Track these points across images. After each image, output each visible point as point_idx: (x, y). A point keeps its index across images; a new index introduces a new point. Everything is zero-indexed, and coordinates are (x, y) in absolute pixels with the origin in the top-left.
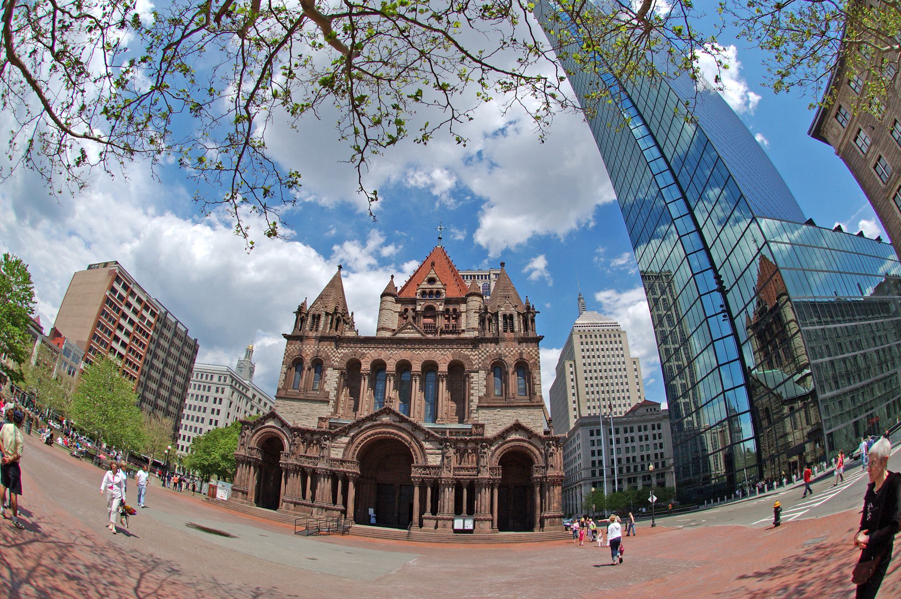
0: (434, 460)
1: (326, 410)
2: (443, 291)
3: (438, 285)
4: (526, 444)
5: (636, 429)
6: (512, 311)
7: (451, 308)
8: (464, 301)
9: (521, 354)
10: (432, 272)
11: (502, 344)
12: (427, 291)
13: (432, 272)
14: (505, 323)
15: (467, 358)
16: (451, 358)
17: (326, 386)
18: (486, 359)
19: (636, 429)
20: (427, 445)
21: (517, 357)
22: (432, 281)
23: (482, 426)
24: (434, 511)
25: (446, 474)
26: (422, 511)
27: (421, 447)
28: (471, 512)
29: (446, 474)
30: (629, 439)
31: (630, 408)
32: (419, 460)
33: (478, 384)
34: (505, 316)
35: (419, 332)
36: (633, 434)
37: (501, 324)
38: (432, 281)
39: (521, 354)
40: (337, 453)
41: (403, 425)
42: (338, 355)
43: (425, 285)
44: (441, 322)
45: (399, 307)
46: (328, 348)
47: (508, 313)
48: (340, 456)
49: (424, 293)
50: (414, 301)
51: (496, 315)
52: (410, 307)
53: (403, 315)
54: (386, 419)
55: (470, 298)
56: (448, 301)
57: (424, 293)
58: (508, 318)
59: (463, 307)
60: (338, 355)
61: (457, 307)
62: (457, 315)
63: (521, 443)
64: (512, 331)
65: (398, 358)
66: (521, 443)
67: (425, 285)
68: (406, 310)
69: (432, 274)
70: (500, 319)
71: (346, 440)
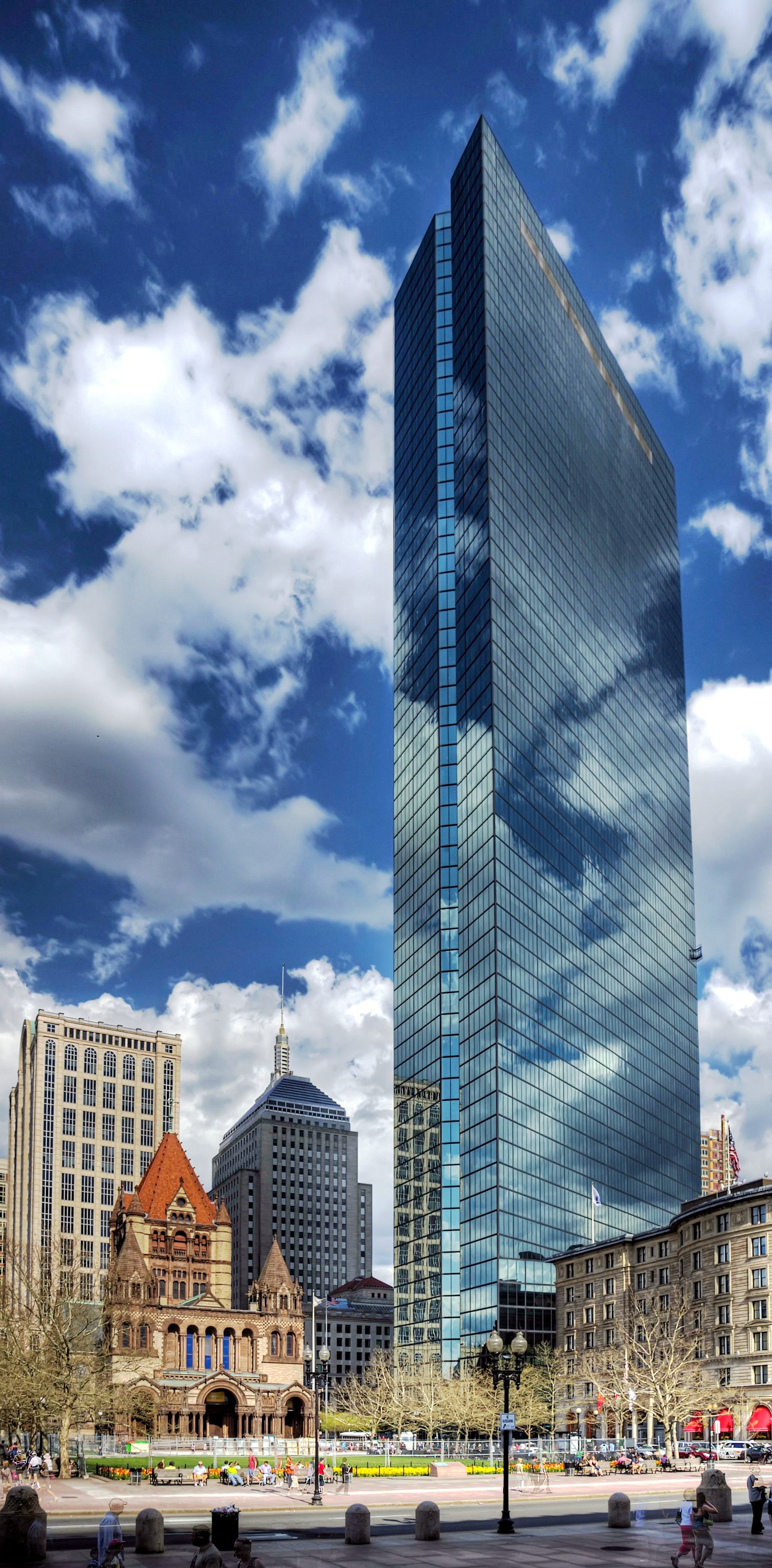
0: (251, 1402)
1: (157, 1363)
2: (194, 1216)
3: (188, 1209)
5: (354, 1328)
6: (287, 1293)
7: (201, 1233)
8: (214, 1229)
9: (291, 1327)
10: (182, 1191)
11: (279, 1319)
12: (178, 1213)
13: (182, 1191)
14: (281, 1302)
15: (255, 1326)
16: (243, 1327)
17: (154, 1346)
19: (354, 1328)
20: (248, 1393)
21: (288, 1329)
22: (182, 1201)
23: (266, 1376)
24: (250, 1432)
25: (259, 1412)
26: (244, 1432)
27: (244, 1395)
28: (270, 1432)
29: (259, 1412)
30: (343, 1342)
31: (344, 1282)
32: (241, 1402)
33: (263, 1345)
34: (281, 1296)
35: (217, 1300)
36: (349, 1336)
37: (278, 1303)
38: (182, 1201)
39: (291, 1327)
40: (192, 1401)
41: (232, 1381)
42: (161, 1319)
43: (174, 1207)
44: (190, 1250)
45: (148, 1229)
46: (151, 1315)
47: (284, 1294)
48: (195, 1403)
49: (174, 1214)
50: (164, 1224)
51: (276, 1293)
52: (160, 1228)
53: (154, 1236)
54: (220, 1377)
55: (220, 1228)
56: (198, 1228)
57: (174, 1214)
59: (213, 1236)
60: (161, 1319)
61: (208, 1233)
62: (208, 1243)
64: (286, 1308)
65: (208, 1325)
67: (174, 1207)
68: (156, 1232)
69: (182, 1193)
70: (278, 1299)
71: (196, 1391)
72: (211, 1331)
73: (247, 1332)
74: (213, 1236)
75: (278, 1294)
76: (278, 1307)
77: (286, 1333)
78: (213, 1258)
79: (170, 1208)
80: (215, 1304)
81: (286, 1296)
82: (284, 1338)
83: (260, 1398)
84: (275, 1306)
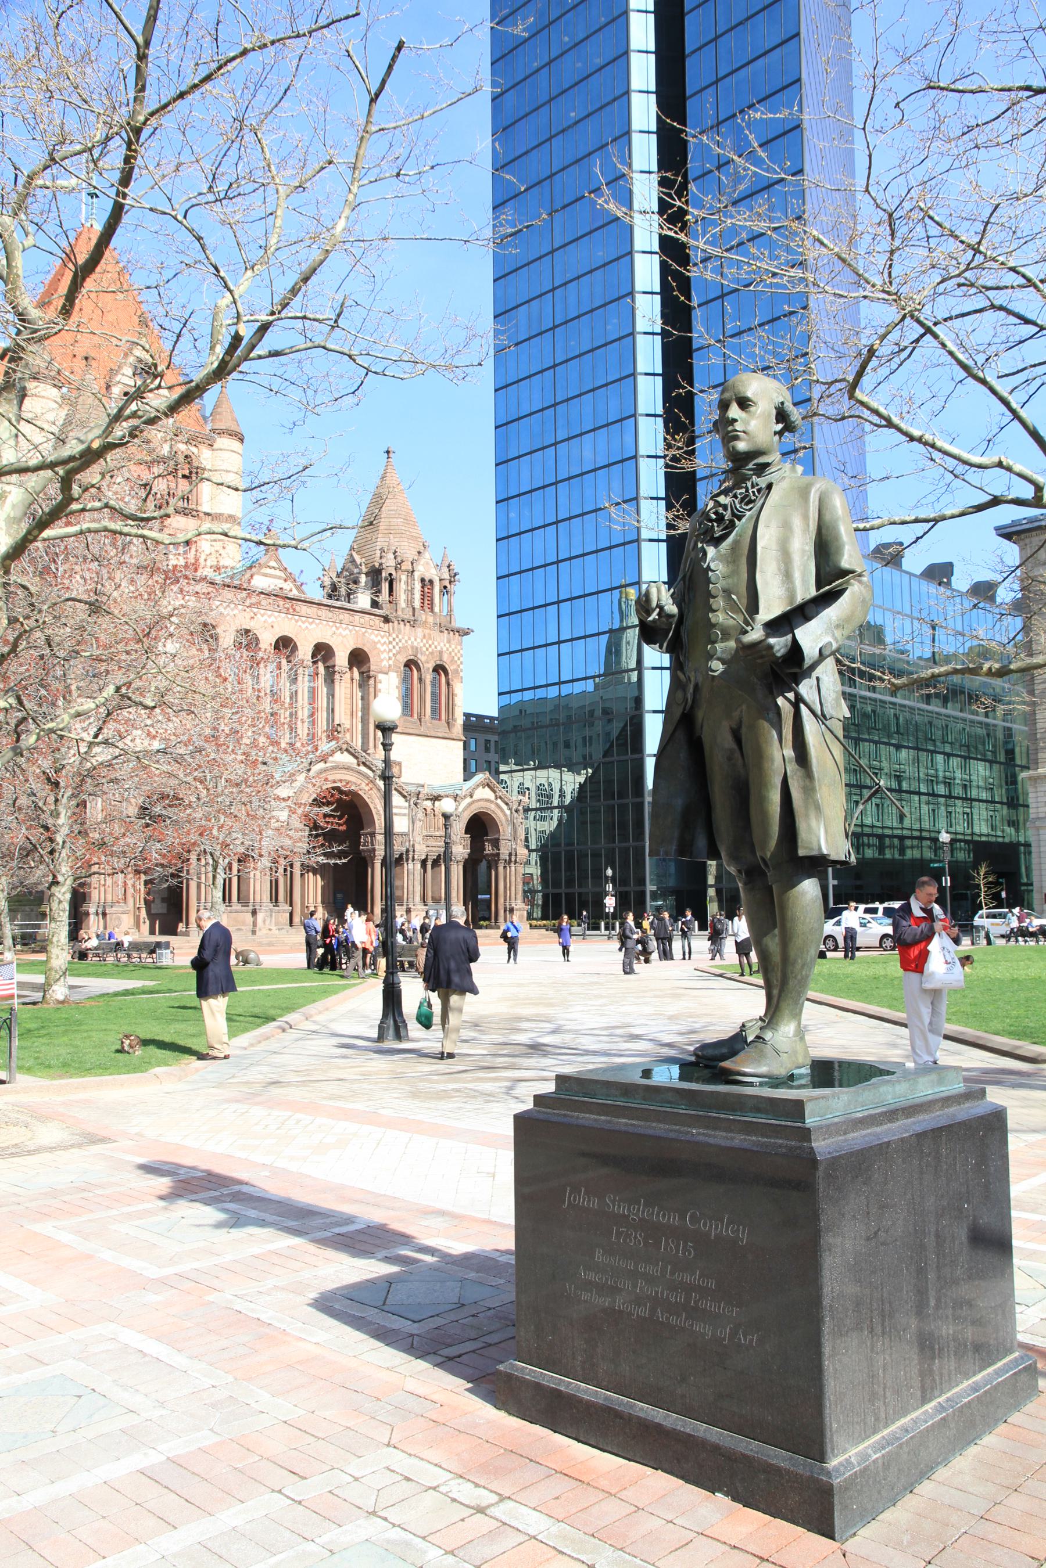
4: (493, 807)
9: (441, 652)
11: (420, 631)
18: (399, 652)
34: (423, 580)
37: (417, 596)
39: (441, 652)
41: (362, 768)
58: (426, 584)
61: (194, 450)
63: (488, 805)
66: (488, 805)
70: (418, 586)
72: (285, 644)
73: (358, 658)
74: (205, 457)
75: (417, 575)
76: (417, 604)
77: (431, 666)
78: (205, 508)
79: (118, 378)
80: (288, 586)
81: (431, 582)
82: (428, 677)
83: (421, 815)
84: (410, 602)
